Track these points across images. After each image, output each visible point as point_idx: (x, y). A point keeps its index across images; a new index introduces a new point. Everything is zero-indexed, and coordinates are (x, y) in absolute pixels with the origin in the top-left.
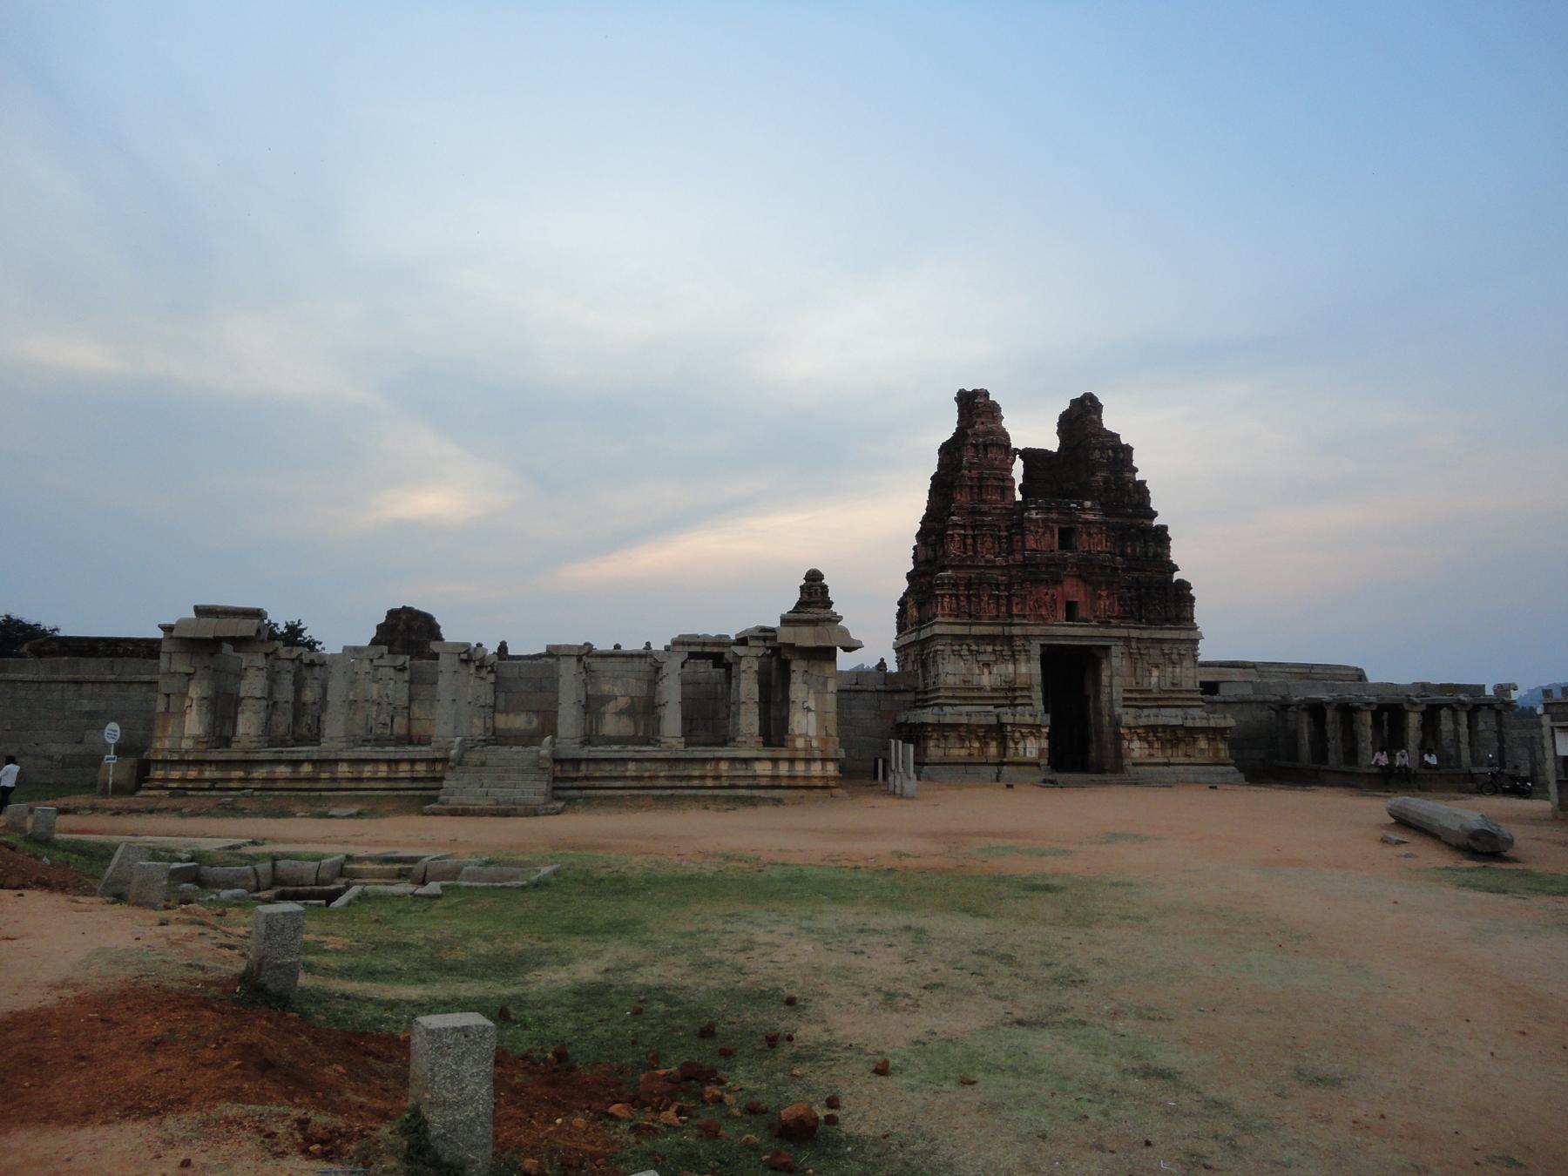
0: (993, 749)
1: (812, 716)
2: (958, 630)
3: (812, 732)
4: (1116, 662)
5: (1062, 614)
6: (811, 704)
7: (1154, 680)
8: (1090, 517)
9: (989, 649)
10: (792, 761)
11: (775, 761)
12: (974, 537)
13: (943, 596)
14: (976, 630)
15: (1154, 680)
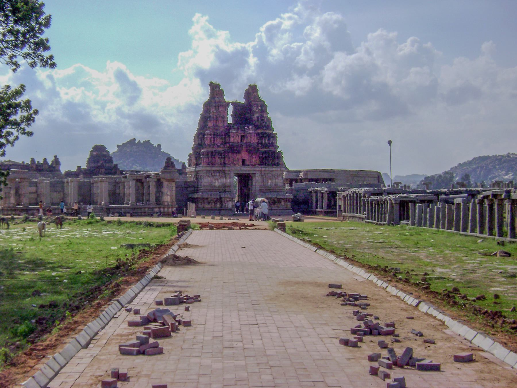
0: (218, 205)
1: (169, 197)
2: (208, 169)
3: (169, 200)
4: (257, 178)
5: (241, 163)
6: (169, 193)
7: (269, 183)
8: (251, 131)
9: (218, 174)
10: (164, 208)
11: (159, 208)
12: (214, 138)
13: (204, 158)
14: (214, 169)
15: (269, 183)
